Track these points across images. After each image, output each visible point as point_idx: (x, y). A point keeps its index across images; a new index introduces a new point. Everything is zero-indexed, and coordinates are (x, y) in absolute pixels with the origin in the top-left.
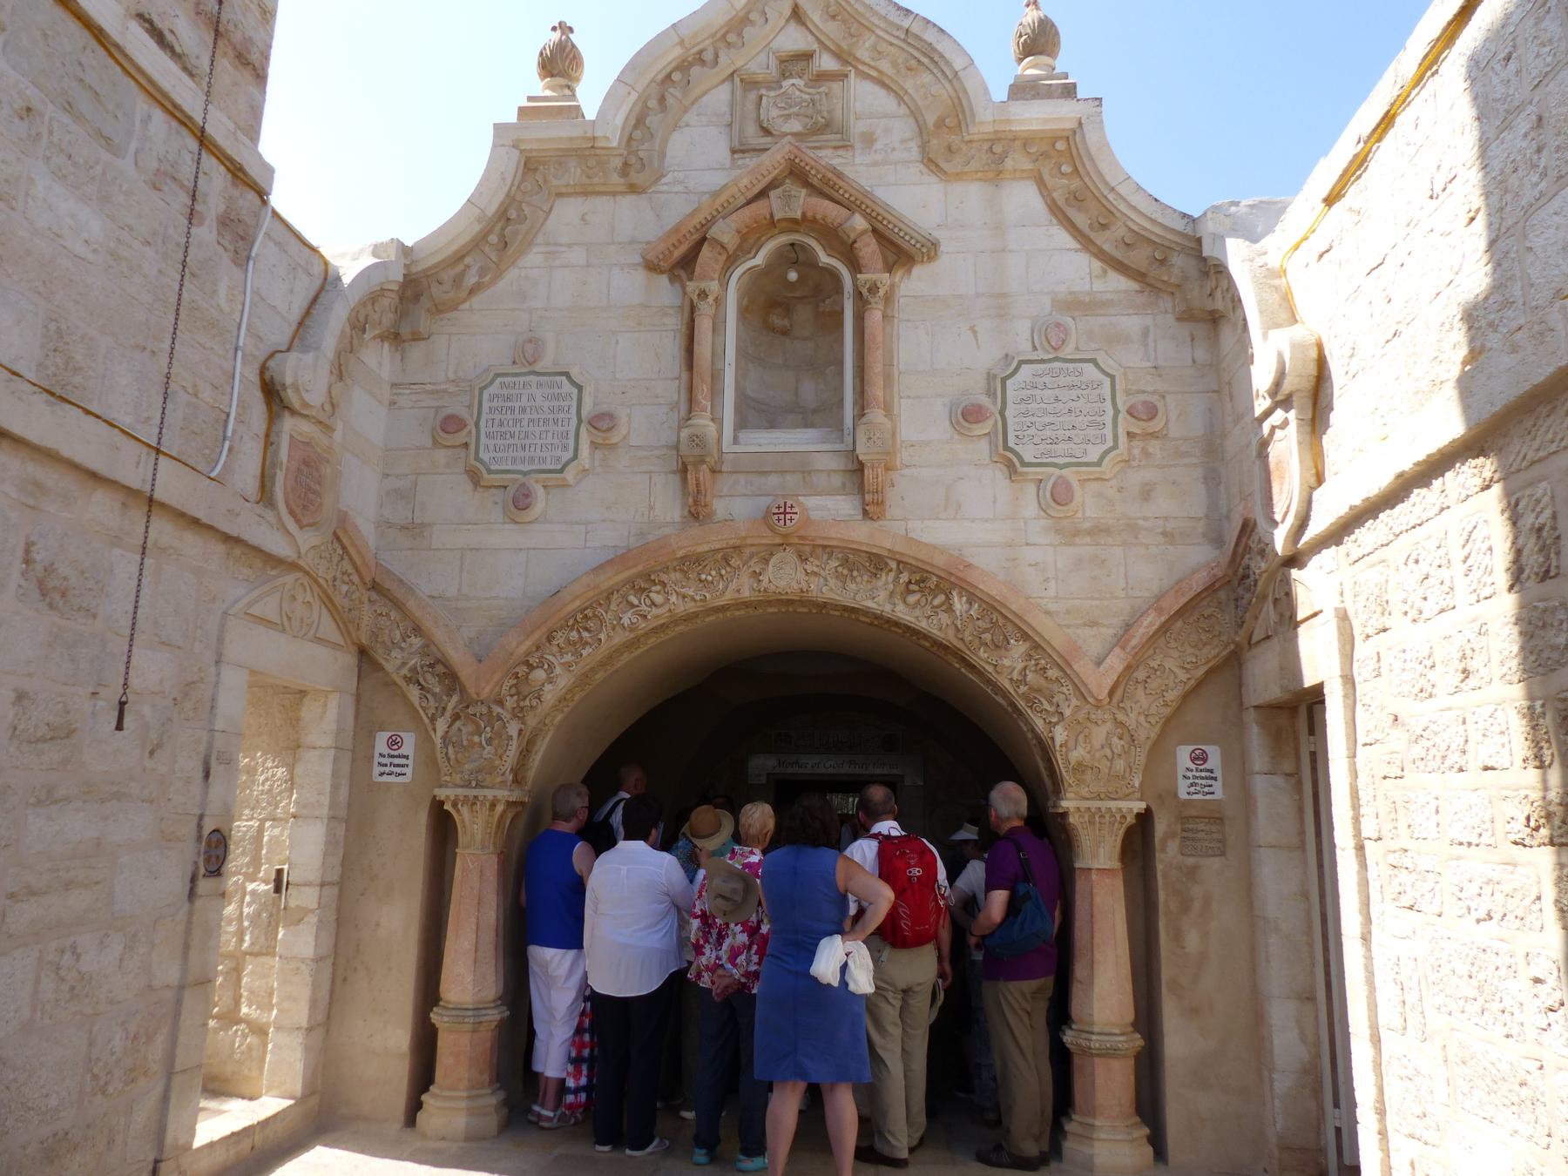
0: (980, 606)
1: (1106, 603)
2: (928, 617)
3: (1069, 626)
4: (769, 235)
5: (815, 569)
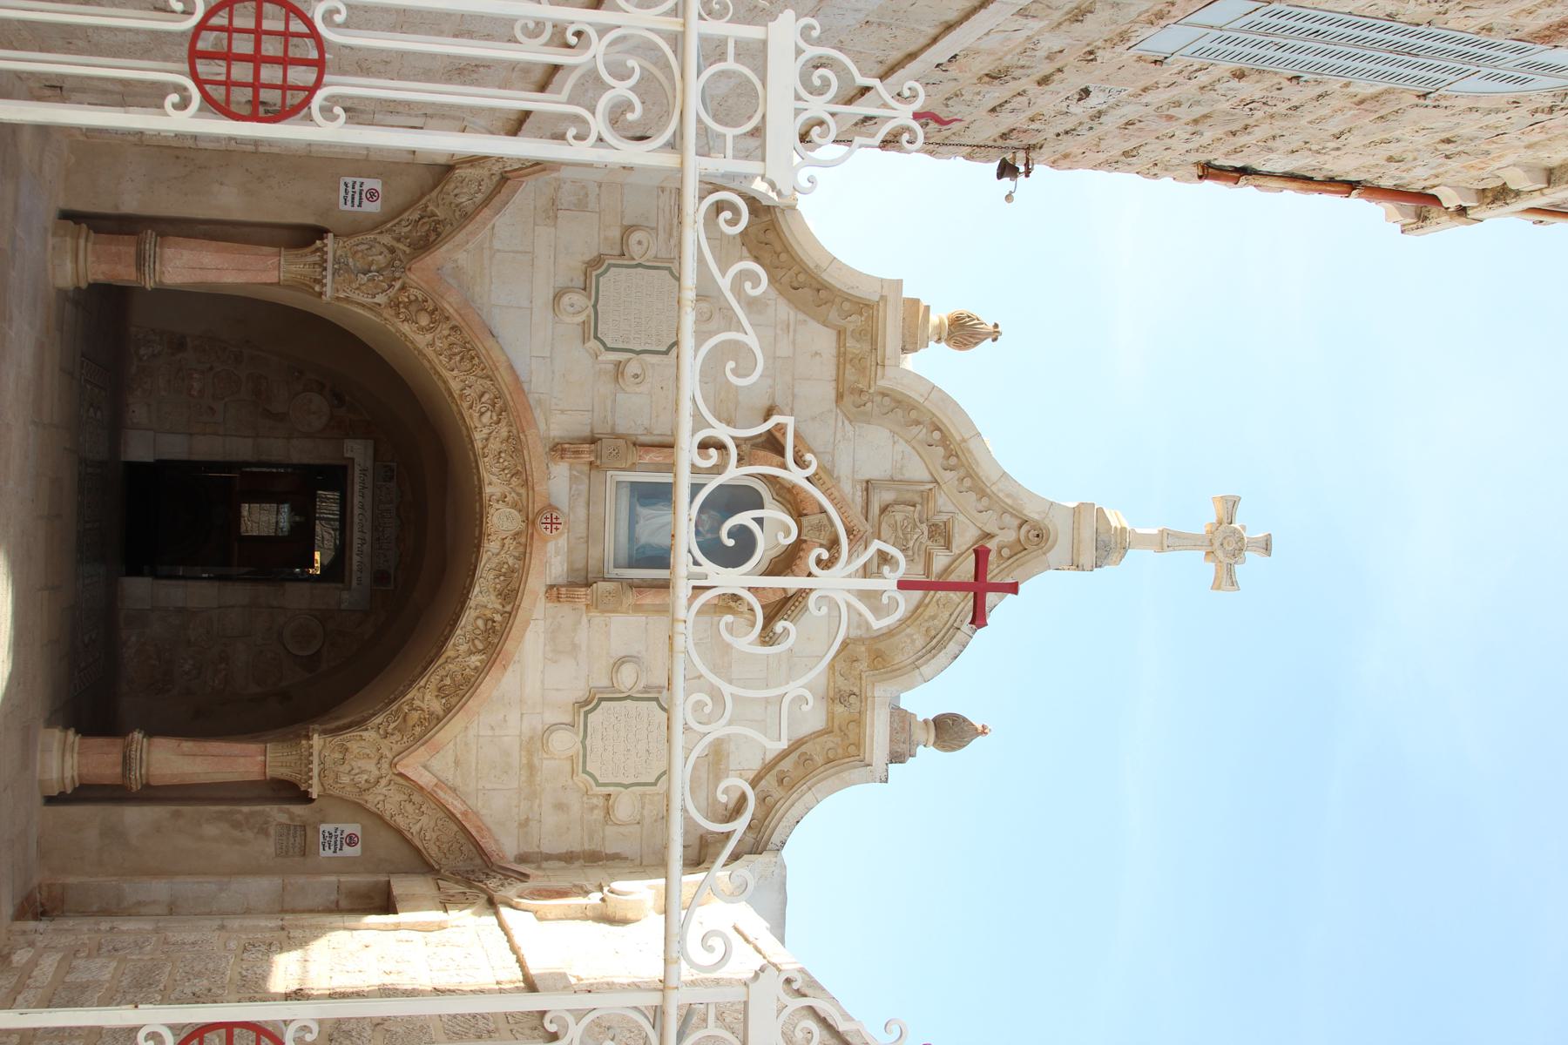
0: (474, 676)
1: (473, 774)
2: (464, 636)
3: (455, 744)
4: (792, 511)
5: (507, 546)
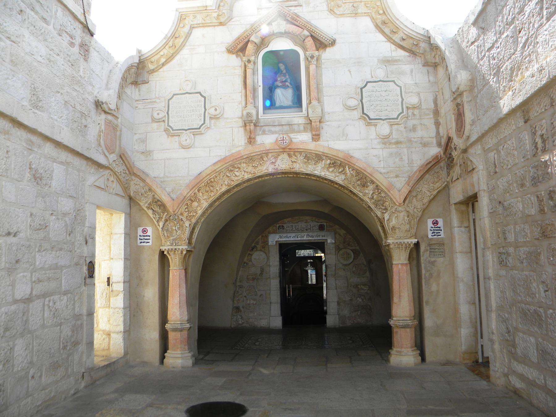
5: (295, 160)
